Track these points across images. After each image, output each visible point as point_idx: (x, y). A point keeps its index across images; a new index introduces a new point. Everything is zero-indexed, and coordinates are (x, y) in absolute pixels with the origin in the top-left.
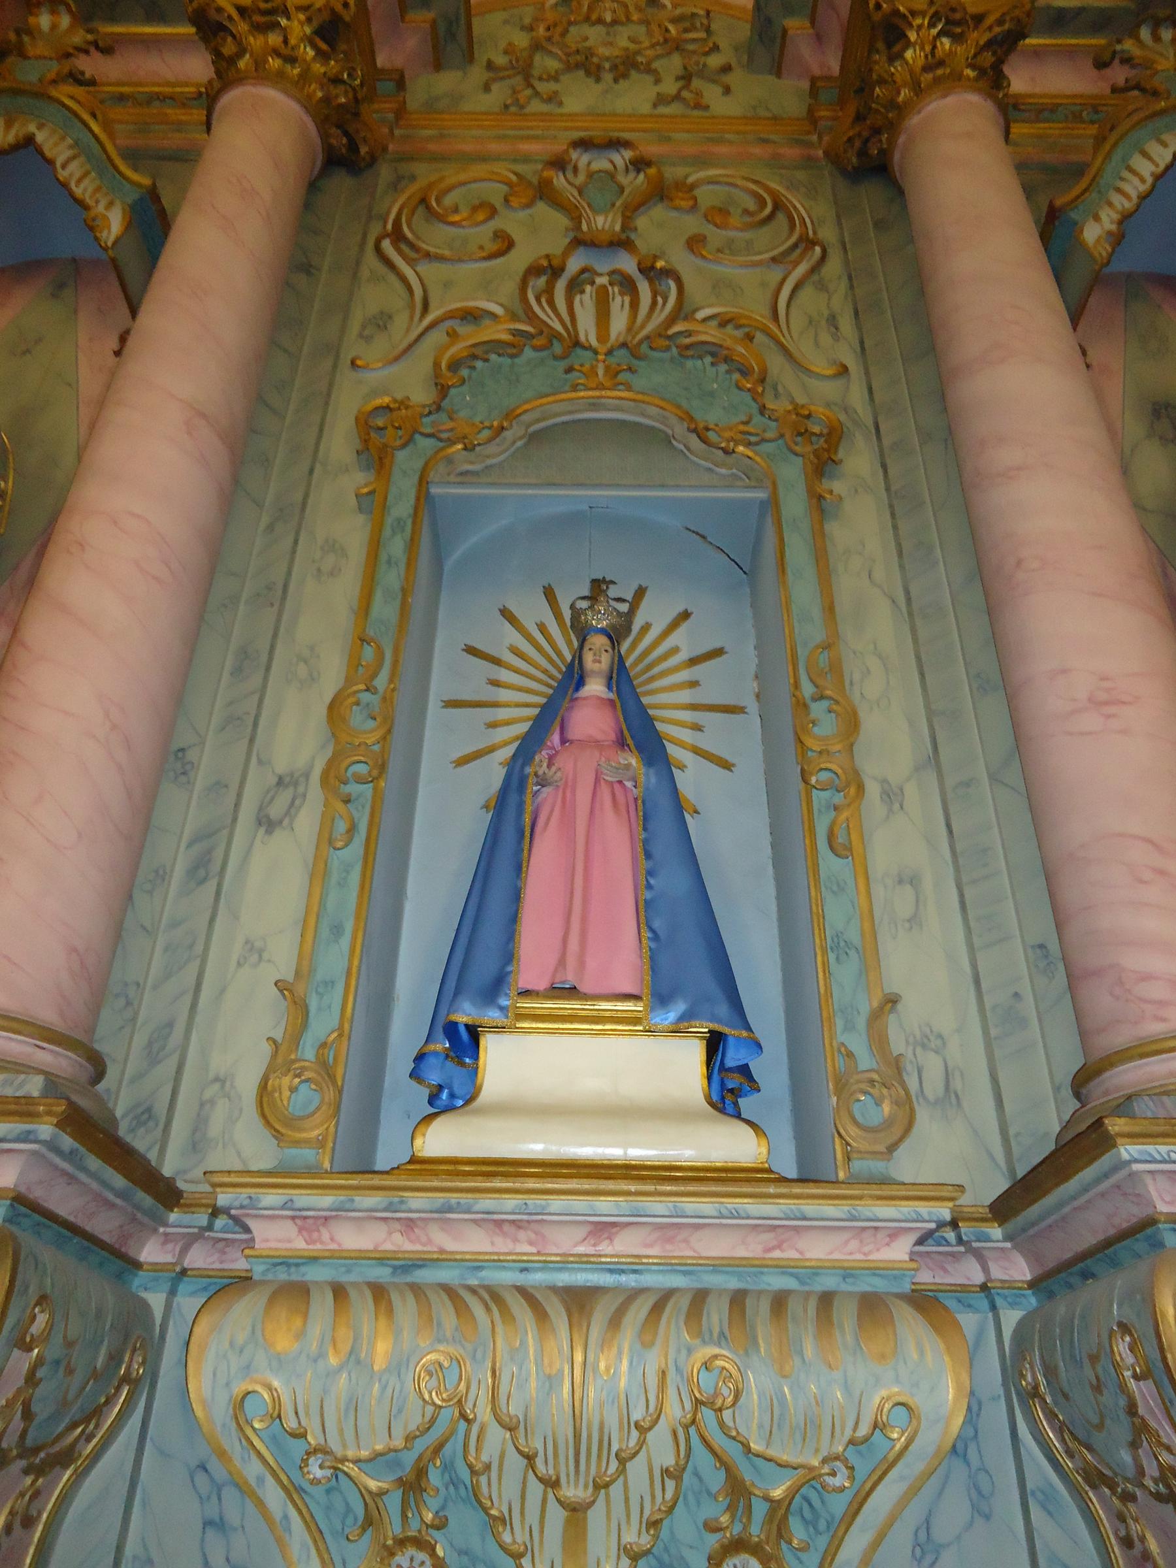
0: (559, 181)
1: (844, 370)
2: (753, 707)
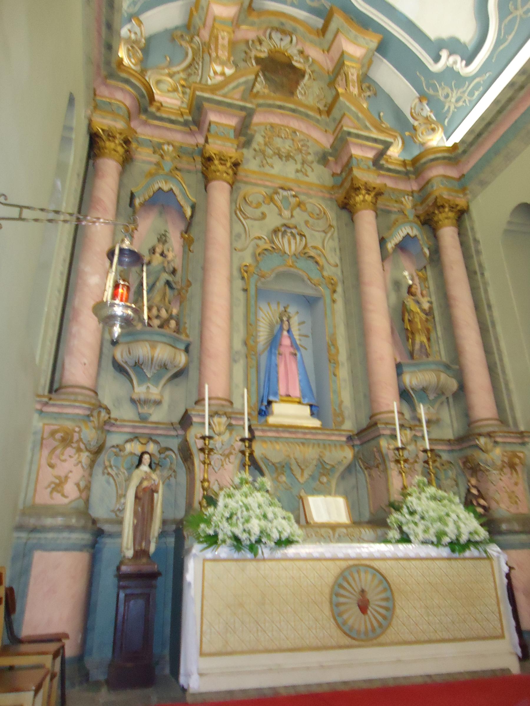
0: (276, 197)
2: (310, 335)
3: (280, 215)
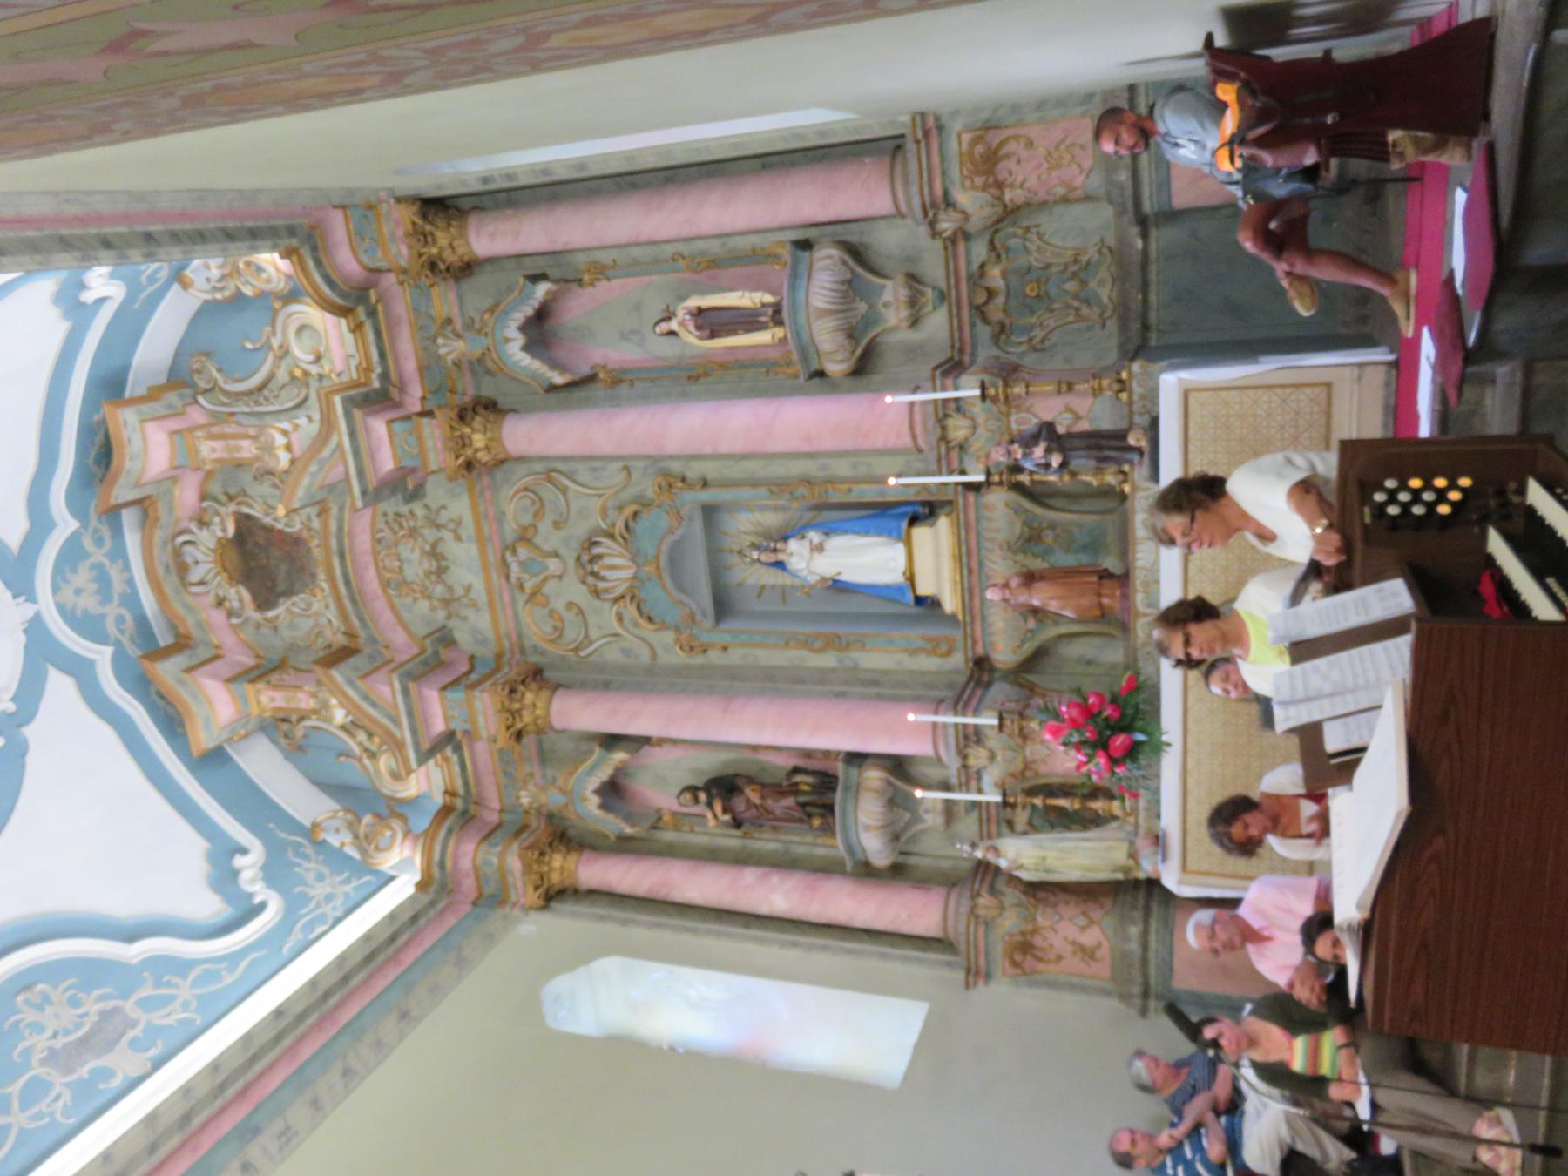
0: (528, 586)
3: (560, 577)
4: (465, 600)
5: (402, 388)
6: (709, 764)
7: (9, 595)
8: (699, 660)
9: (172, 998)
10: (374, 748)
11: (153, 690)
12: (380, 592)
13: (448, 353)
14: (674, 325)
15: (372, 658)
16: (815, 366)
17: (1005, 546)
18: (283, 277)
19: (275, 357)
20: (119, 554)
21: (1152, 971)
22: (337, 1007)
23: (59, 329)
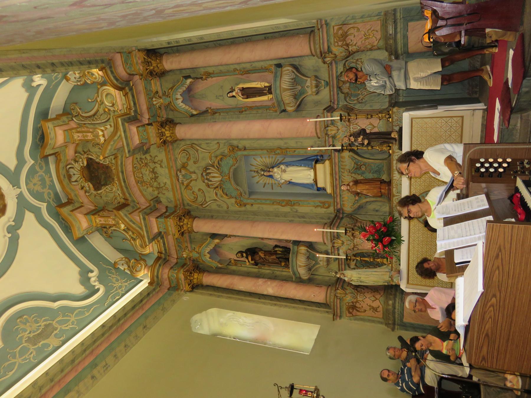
0: (185, 183)
1: (218, 143)
3: (196, 180)
4: (164, 188)
5: (142, 115)
6: (247, 244)
7: (11, 186)
8: (243, 209)
9: (69, 320)
10: (135, 237)
11: (60, 217)
12: (135, 185)
13: (157, 104)
14: (234, 94)
15: (133, 207)
16: (283, 108)
17: (348, 171)
18: (100, 77)
19: (99, 104)
20: (48, 171)
21: (396, 316)
22: (123, 324)
23: (25, 95)
